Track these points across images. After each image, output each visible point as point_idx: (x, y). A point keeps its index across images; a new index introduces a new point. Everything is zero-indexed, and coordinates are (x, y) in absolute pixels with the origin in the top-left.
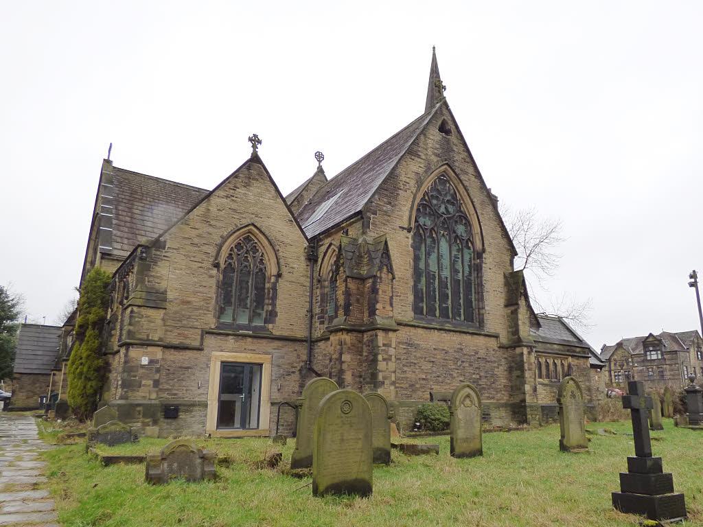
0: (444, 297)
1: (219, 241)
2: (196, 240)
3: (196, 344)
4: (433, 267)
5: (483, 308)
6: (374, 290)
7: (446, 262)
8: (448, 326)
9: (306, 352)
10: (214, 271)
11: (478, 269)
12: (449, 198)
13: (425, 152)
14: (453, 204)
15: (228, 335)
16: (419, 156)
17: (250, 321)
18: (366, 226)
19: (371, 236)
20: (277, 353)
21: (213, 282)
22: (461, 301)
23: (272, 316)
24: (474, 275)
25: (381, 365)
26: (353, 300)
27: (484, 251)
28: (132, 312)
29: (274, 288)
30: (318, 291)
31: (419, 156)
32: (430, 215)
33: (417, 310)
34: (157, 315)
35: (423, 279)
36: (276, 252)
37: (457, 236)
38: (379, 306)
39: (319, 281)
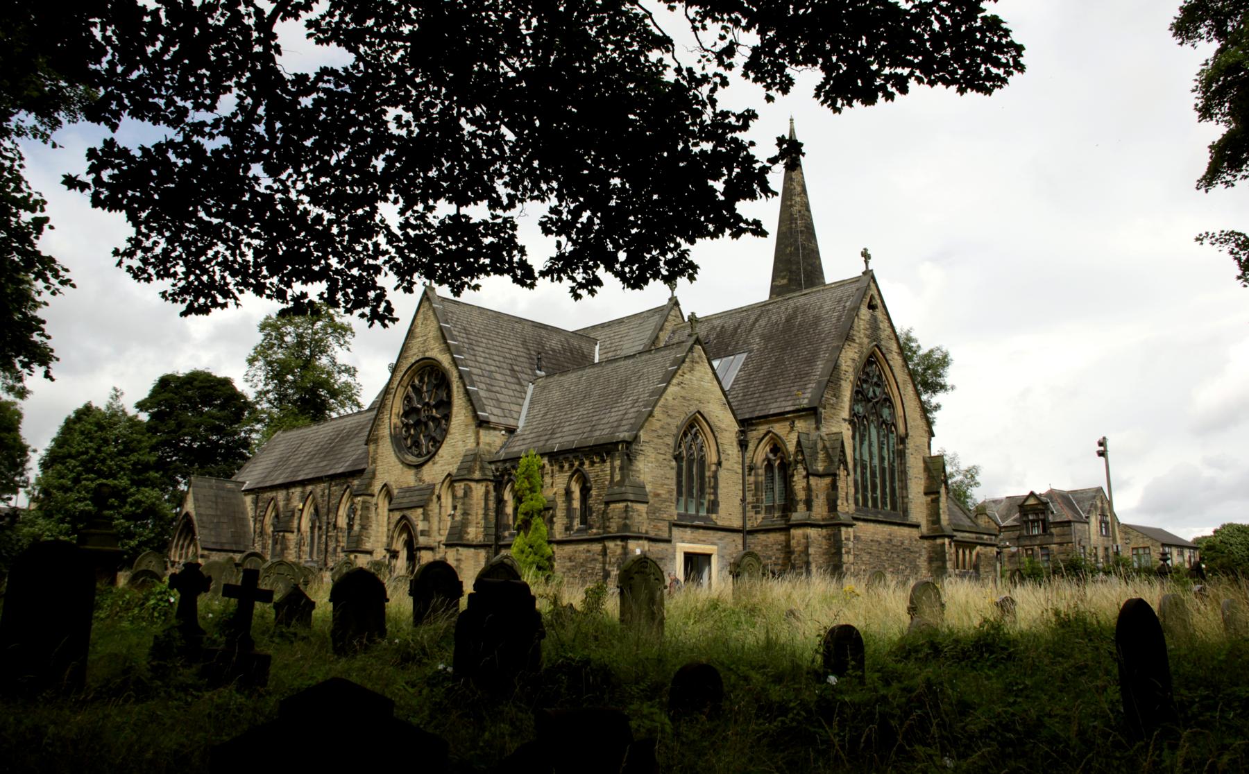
1: (675, 431)
2: (660, 432)
3: (666, 536)
4: (866, 457)
6: (834, 486)
7: (875, 450)
8: (881, 518)
9: (741, 542)
10: (674, 463)
11: (901, 454)
12: (875, 380)
14: (879, 386)
15: (685, 526)
17: (697, 511)
18: (818, 423)
19: (824, 430)
20: (721, 544)
21: (673, 474)
23: (714, 506)
25: (845, 558)
26: (814, 494)
27: (907, 435)
28: (627, 506)
29: (715, 477)
30: (752, 479)
31: (854, 341)
32: (861, 401)
33: (856, 503)
34: (642, 508)
36: (716, 438)
37: (884, 422)
38: (839, 502)
39: (751, 469)
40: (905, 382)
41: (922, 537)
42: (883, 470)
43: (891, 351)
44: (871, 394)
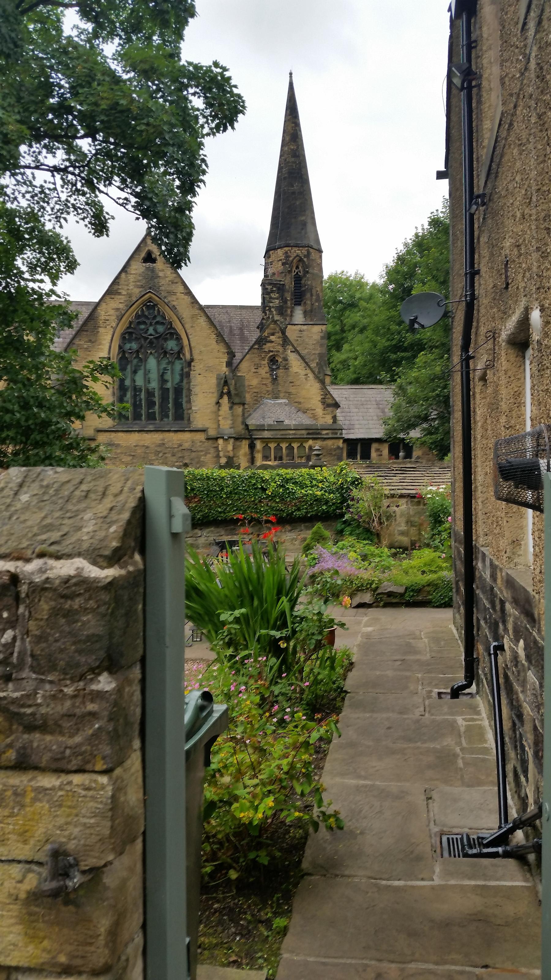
0: (151, 404)
5: (191, 408)
7: (154, 375)
11: (186, 375)
13: (126, 287)
14: (163, 324)
16: (120, 294)
22: (170, 405)
24: (185, 381)
27: (192, 360)
31: (120, 294)
35: (129, 395)
37: (165, 353)
40: (193, 317)
41: (208, 439)
42: (164, 392)
43: (175, 294)
44: (151, 331)
